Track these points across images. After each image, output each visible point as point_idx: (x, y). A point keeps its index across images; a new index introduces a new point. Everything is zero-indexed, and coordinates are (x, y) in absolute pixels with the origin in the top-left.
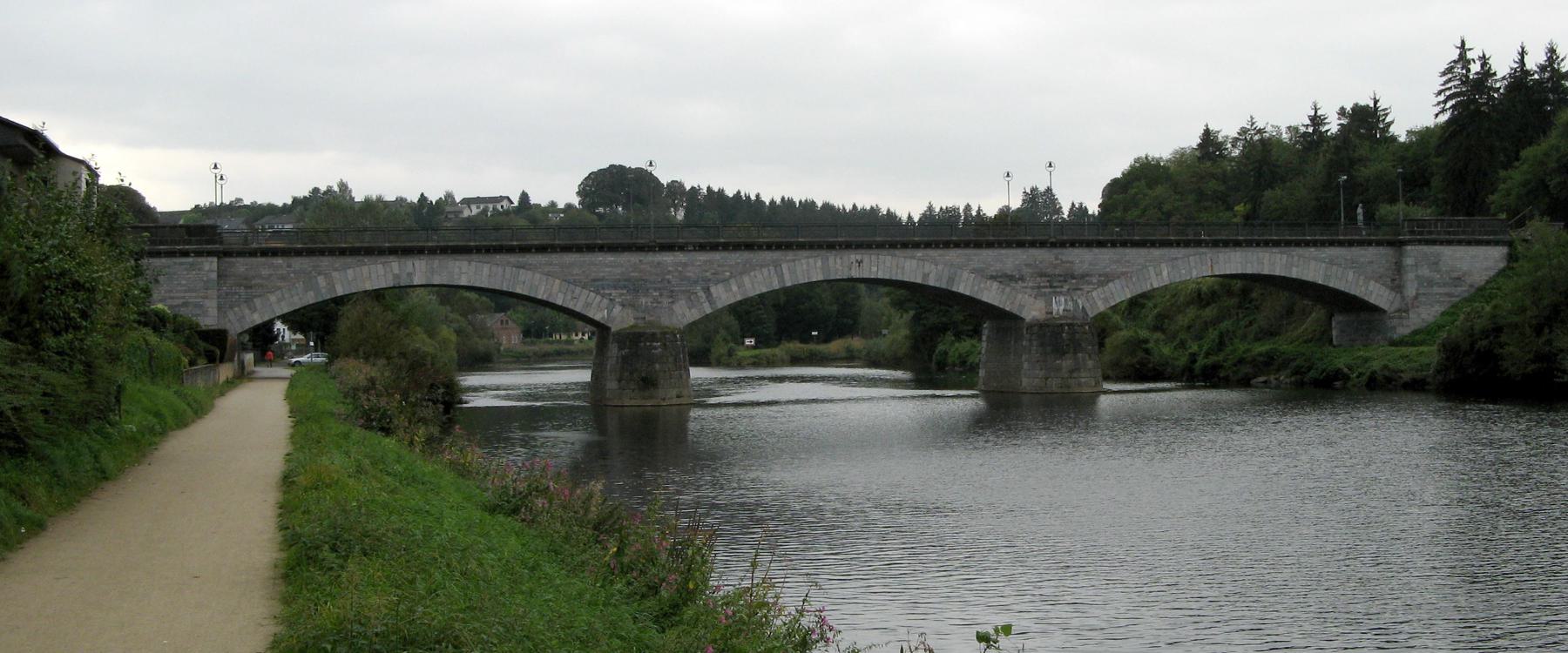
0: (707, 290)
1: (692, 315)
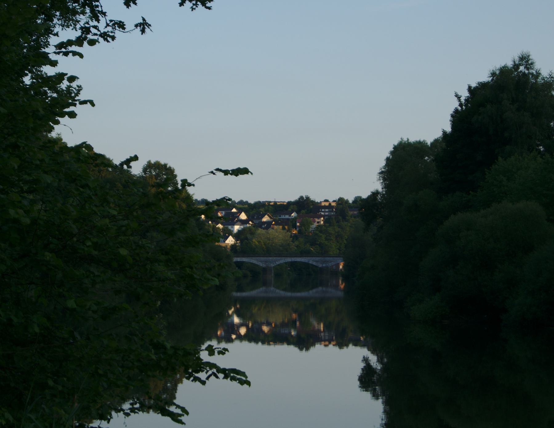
0: (275, 262)
1: (274, 265)
